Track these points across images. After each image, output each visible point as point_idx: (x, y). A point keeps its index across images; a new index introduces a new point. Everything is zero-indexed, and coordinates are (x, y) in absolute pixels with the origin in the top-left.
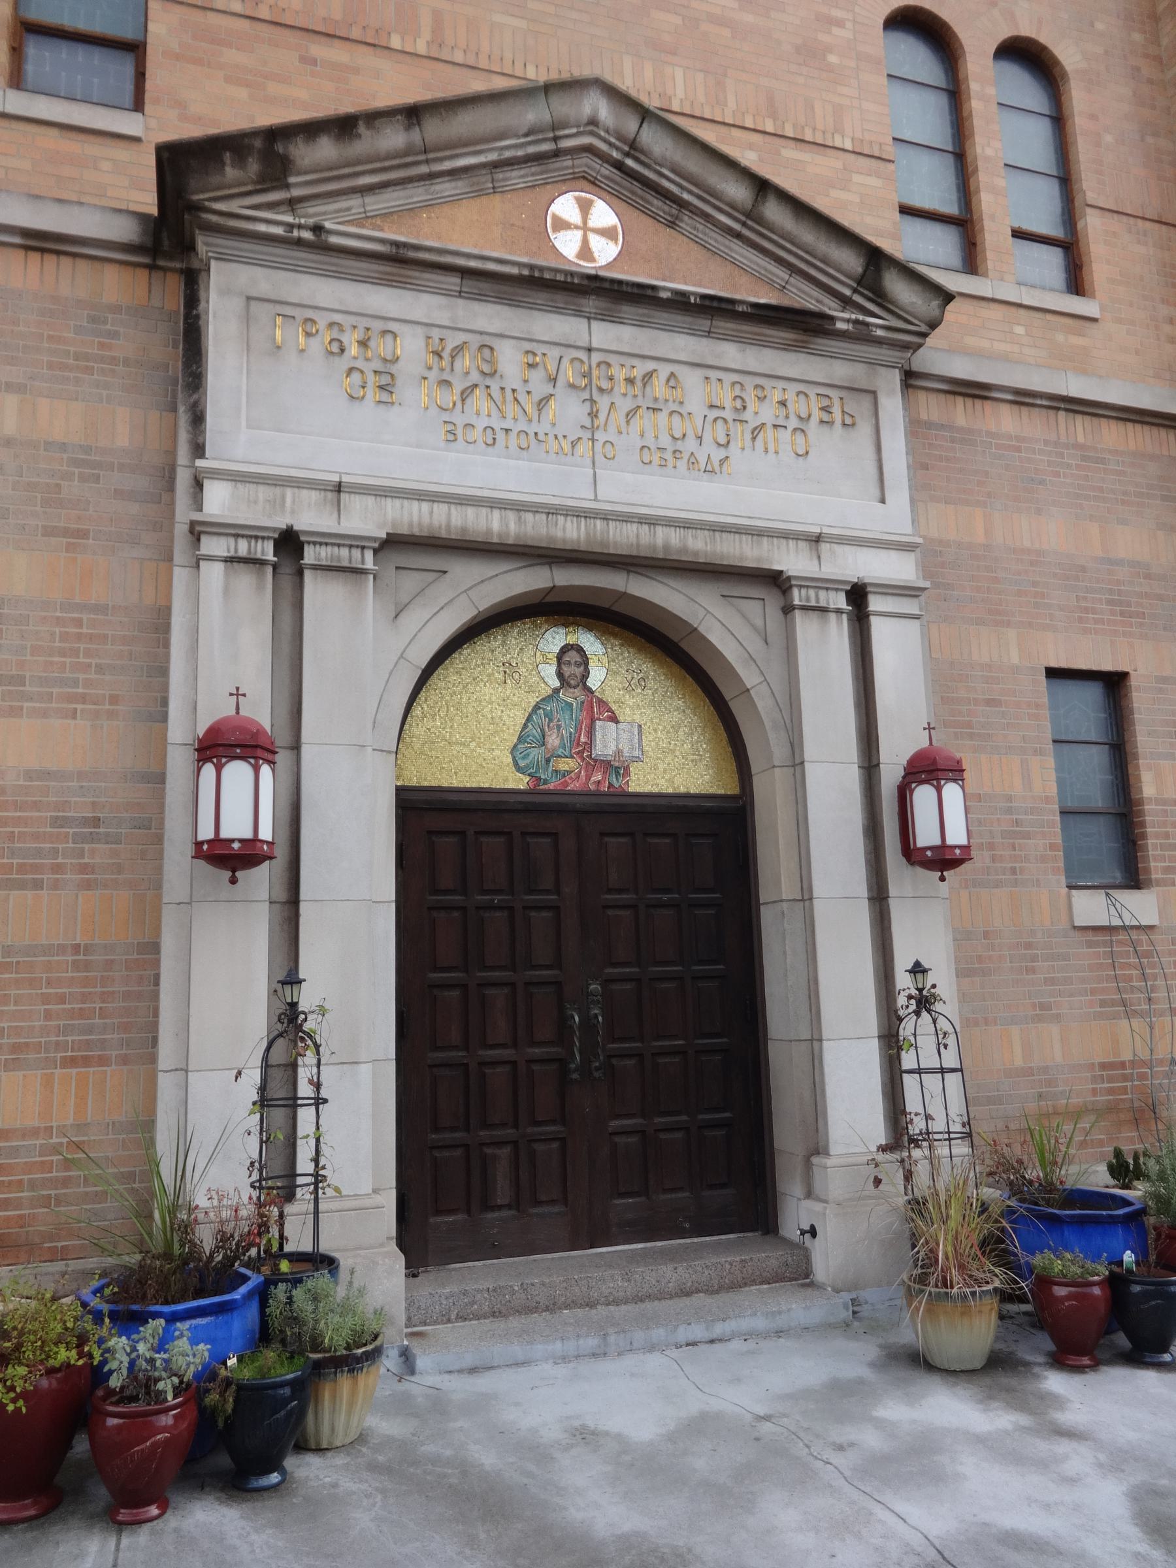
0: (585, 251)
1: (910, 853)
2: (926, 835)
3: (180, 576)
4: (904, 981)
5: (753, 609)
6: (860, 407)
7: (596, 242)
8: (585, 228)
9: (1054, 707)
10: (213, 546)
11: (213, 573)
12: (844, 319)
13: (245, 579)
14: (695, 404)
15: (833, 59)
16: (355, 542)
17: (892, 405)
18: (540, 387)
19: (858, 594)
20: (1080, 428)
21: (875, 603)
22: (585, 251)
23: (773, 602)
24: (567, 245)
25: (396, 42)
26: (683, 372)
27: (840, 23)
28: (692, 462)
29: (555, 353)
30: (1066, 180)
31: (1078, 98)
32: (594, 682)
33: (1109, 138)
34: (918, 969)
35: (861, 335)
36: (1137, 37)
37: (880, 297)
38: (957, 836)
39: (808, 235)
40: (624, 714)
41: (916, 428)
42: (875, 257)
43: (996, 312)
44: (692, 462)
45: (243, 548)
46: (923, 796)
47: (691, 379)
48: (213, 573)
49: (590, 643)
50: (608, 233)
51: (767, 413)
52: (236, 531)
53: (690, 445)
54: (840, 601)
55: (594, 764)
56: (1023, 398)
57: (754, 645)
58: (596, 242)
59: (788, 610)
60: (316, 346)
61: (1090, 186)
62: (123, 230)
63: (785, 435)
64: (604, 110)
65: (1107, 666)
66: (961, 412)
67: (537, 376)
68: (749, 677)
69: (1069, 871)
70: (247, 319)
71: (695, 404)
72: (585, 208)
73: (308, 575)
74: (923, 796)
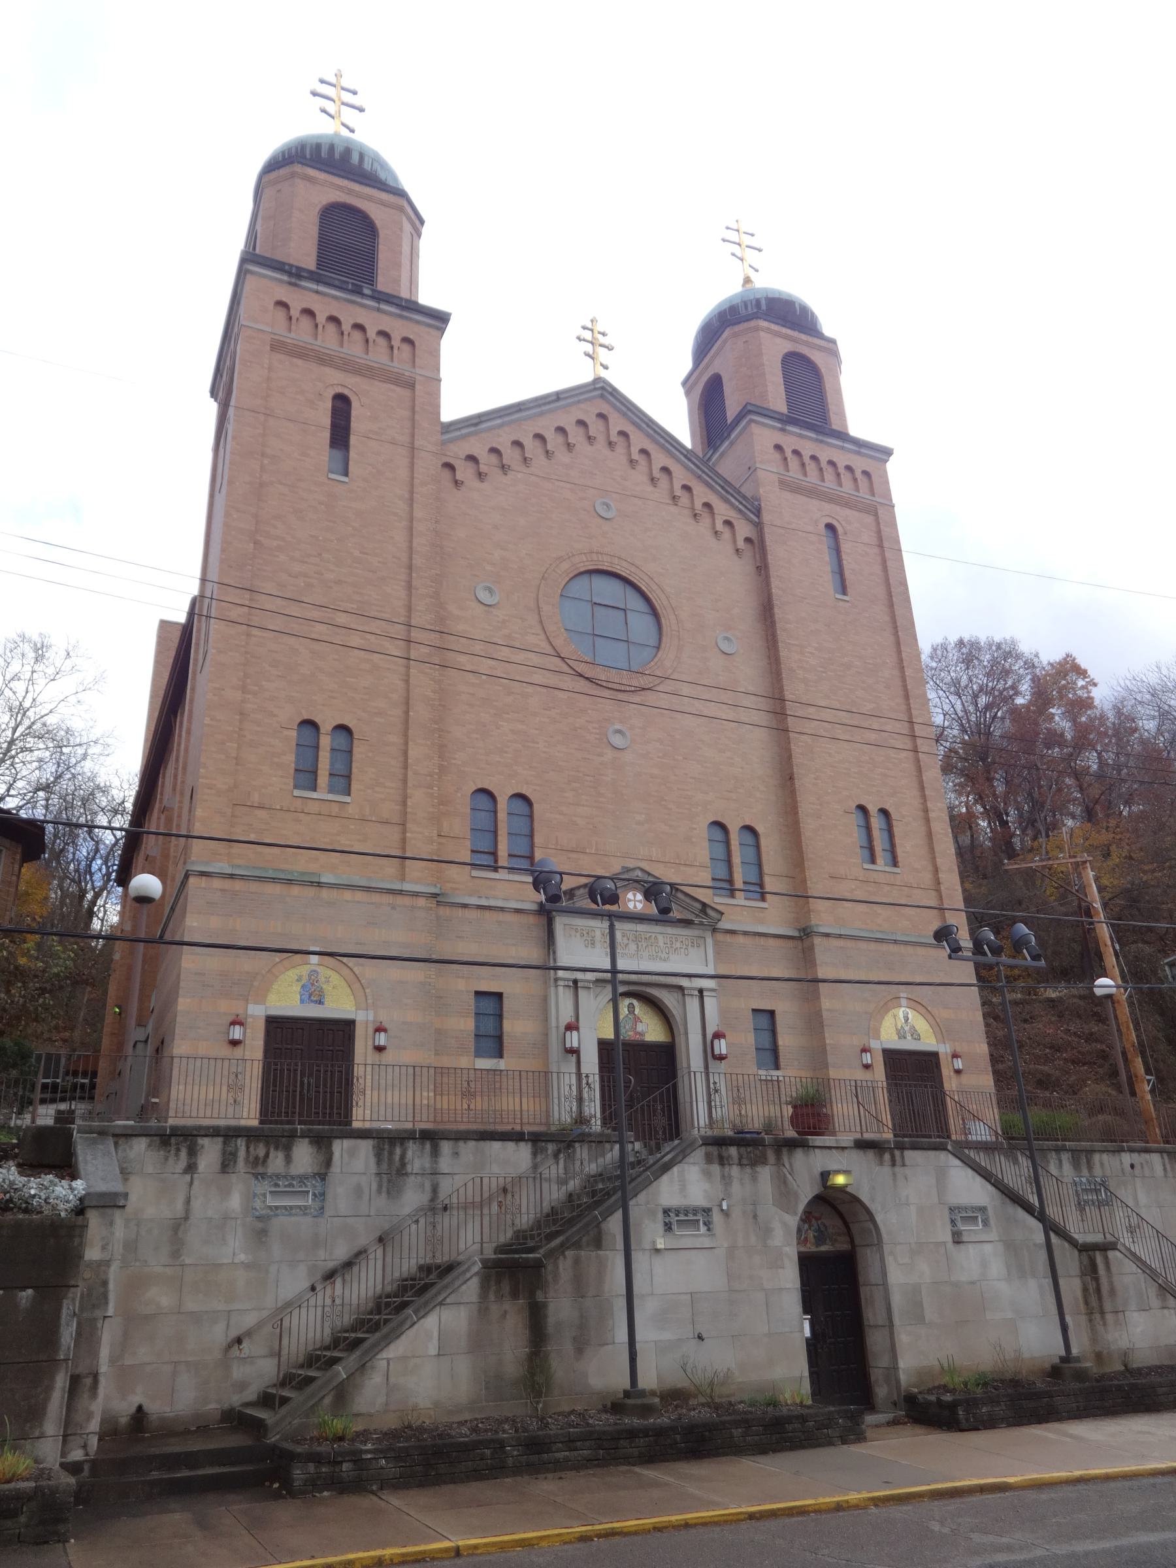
0: (635, 907)
1: (715, 1057)
2: (717, 1052)
3: (553, 989)
4: (712, 1086)
5: (675, 994)
6: (701, 941)
7: (637, 904)
8: (635, 901)
9: (754, 1019)
10: (561, 983)
11: (561, 989)
12: (697, 920)
13: (567, 990)
14: (661, 944)
15: (694, 840)
16: (589, 981)
17: (709, 941)
18: (626, 941)
19: (701, 991)
20: (762, 941)
21: (705, 993)
22: (635, 907)
23: (679, 995)
24: (631, 905)
25: (588, 851)
26: (659, 936)
27: (695, 829)
28: (661, 959)
29: (628, 933)
30: (760, 865)
31: (763, 842)
32: (636, 1013)
33: (772, 853)
34: (715, 1083)
35: (701, 924)
36: (781, 820)
37: (706, 914)
38: (724, 1051)
39: (688, 900)
40: (644, 1021)
41: (716, 943)
42: (704, 905)
43: (739, 909)
44: (661, 959)
45: (566, 983)
46: (716, 1042)
47: (660, 937)
48: (561, 989)
49: (635, 1002)
50: (640, 901)
51: (678, 945)
52: (565, 979)
53: (660, 954)
54: (696, 993)
55: (637, 1033)
56: (746, 933)
57: (675, 1003)
58: (637, 904)
59: (684, 995)
60: (578, 934)
61: (766, 869)
62: (534, 907)
63: (682, 950)
64: (640, 873)
65: (769, 1008)
66: (728, 938)
67: (625, 938)
68: (675, 1012)
69: (758, 1064)
70: (565, 929)
71: (661, 944)
72: (635, 895)
73: (579, 989)
74: (716, 1042)
